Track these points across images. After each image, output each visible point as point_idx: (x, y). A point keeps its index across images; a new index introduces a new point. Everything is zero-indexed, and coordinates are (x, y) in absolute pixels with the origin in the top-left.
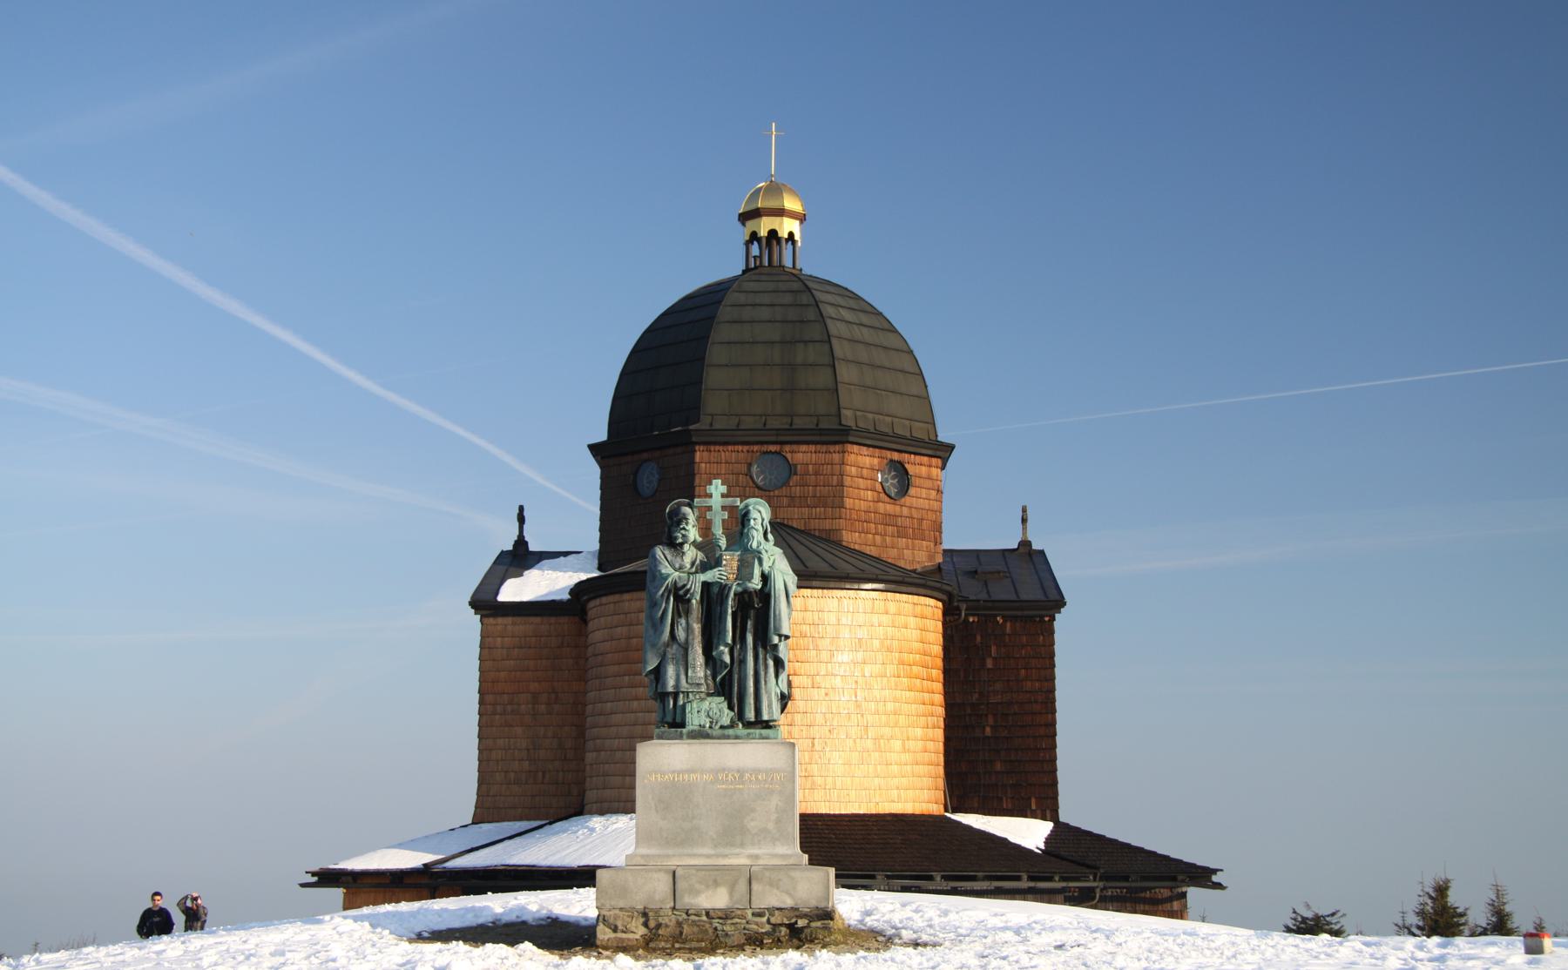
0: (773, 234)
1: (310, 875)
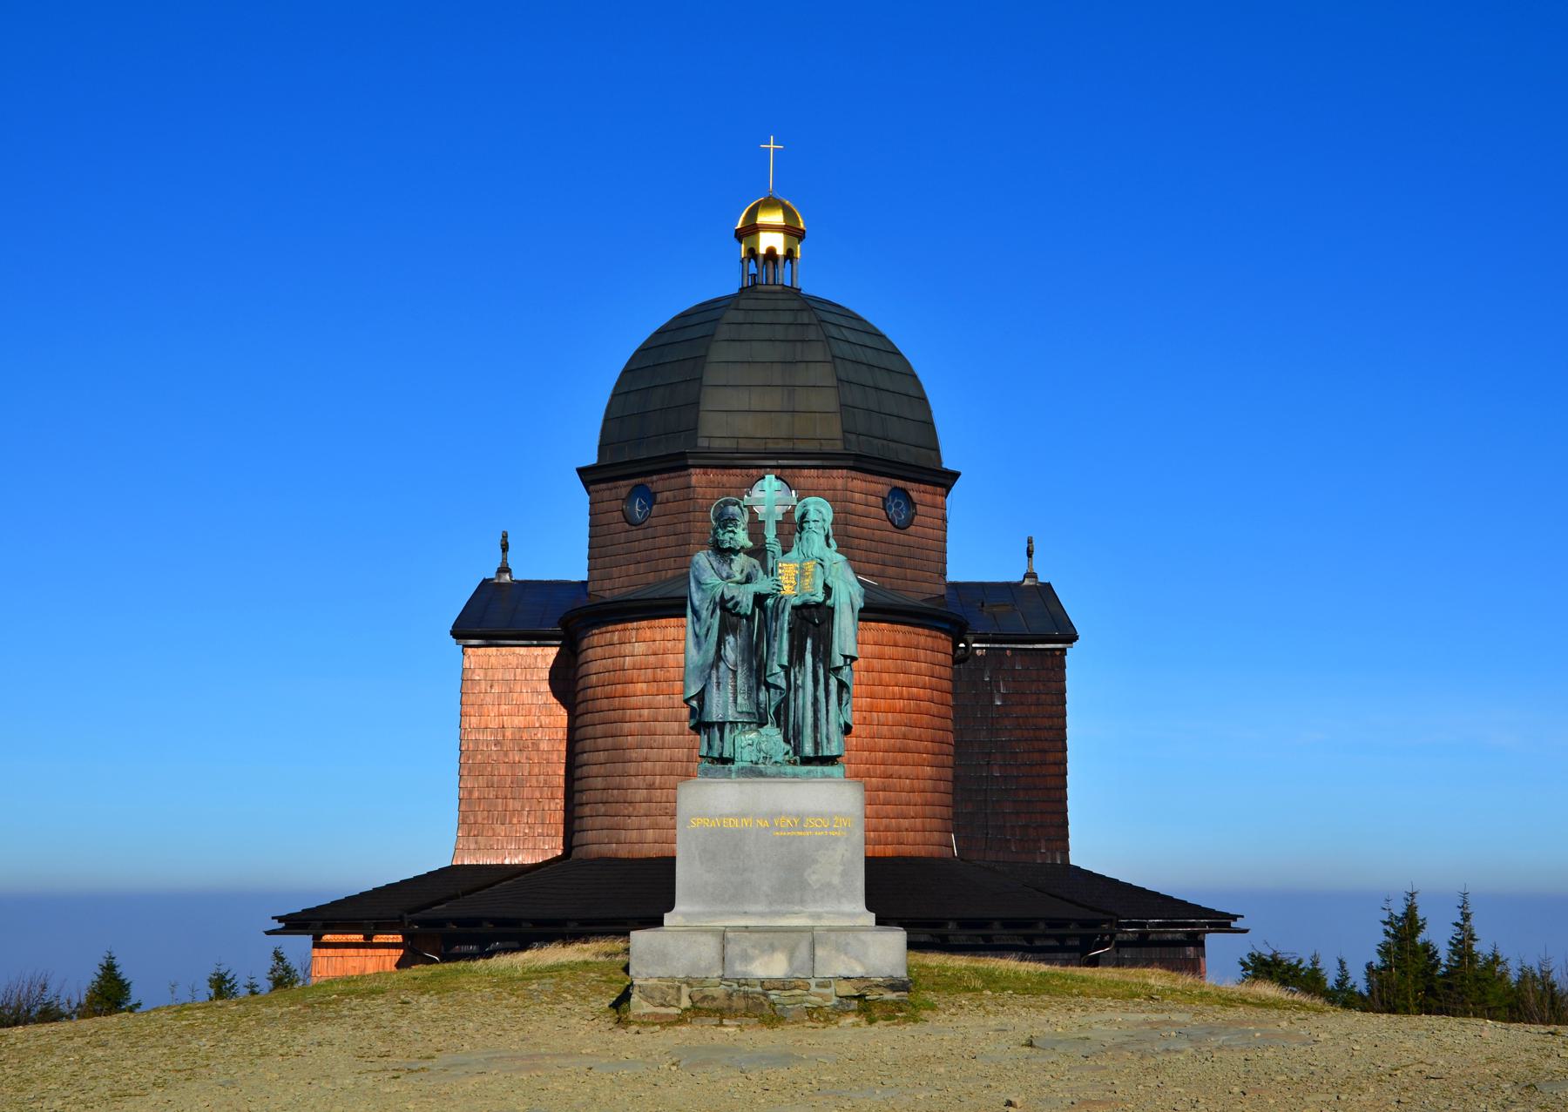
1: (277, 920)
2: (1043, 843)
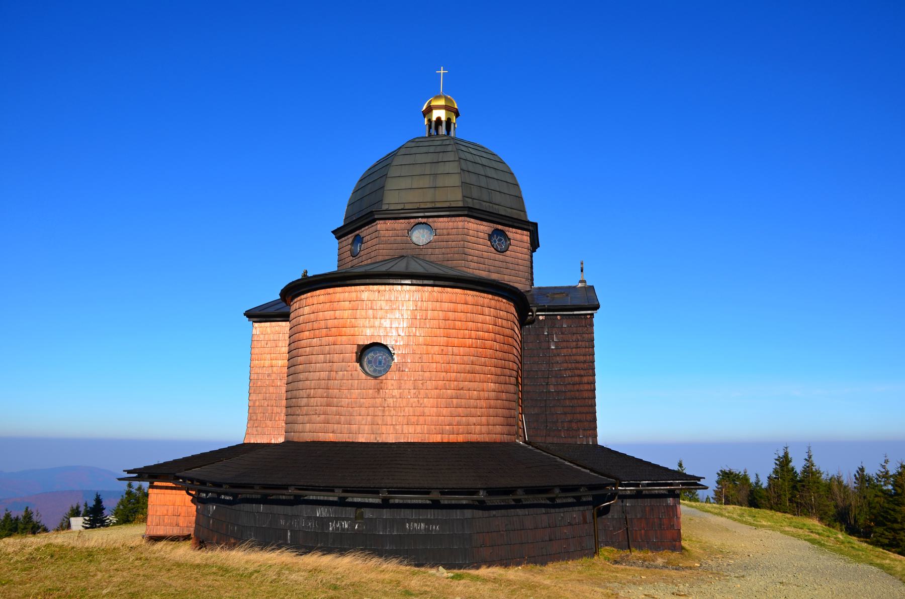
0: (439, 119)
2: (581, 431)
